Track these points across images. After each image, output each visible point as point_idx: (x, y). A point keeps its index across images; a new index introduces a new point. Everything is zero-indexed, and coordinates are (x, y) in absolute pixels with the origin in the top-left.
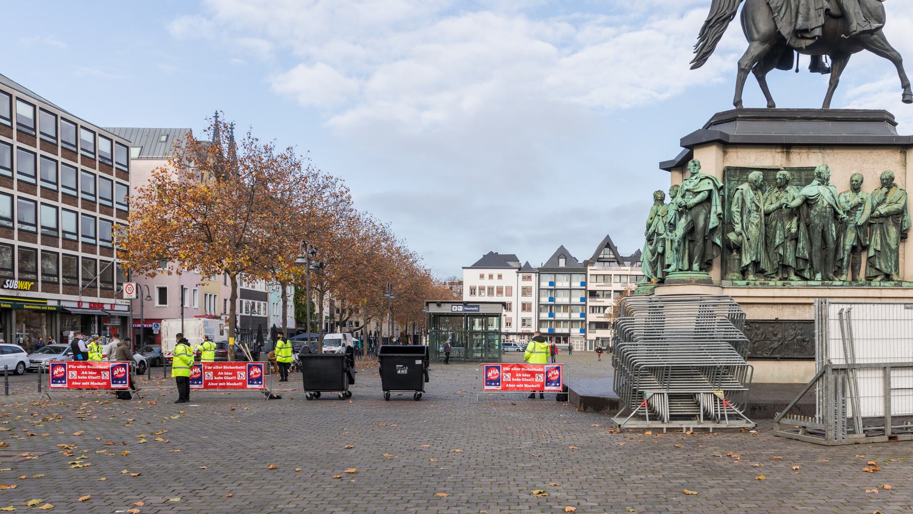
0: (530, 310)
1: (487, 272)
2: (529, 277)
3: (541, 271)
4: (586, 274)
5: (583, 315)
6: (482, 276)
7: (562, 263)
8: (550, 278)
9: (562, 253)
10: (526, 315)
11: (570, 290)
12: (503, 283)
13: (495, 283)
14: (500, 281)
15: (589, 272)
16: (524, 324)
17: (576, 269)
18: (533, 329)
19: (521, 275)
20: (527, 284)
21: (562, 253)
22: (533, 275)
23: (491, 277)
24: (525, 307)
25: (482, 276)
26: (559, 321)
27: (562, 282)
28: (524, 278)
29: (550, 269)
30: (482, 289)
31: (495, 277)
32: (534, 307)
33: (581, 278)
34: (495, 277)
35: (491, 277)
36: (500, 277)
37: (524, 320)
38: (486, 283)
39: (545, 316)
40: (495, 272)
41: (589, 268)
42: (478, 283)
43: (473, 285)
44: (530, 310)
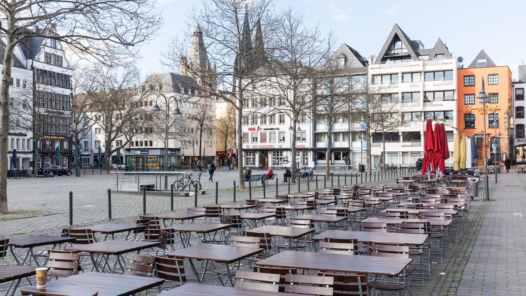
18: (308, 144)
26: (337, 134)
39: (322, 127)
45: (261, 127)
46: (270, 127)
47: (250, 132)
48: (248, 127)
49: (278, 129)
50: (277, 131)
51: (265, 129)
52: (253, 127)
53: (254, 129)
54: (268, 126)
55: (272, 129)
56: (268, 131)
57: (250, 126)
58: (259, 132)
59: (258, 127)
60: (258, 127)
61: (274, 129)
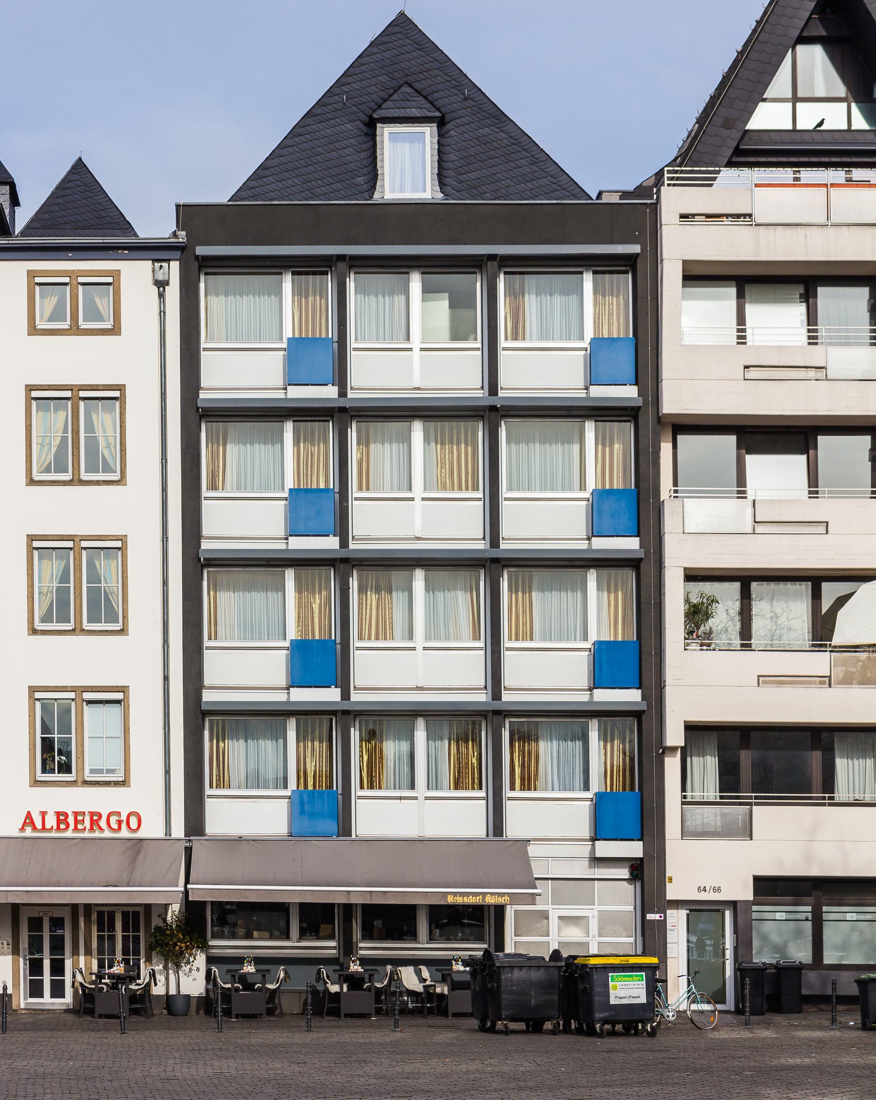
0: (105, 612)
3: (216, 245)
4: (637, 271)
5: (637, 659)
7: (407, 165)
8: (286, 306)
9: (402, 74)
10: (76, 660)
11: (491, 413)
15: (679, 244)
17: (516, 217)
21: (402, 74)
27: (409, 341)
29: (297, 218)
32: (149, 583)
33: (594, 307)
41: (674, 200)
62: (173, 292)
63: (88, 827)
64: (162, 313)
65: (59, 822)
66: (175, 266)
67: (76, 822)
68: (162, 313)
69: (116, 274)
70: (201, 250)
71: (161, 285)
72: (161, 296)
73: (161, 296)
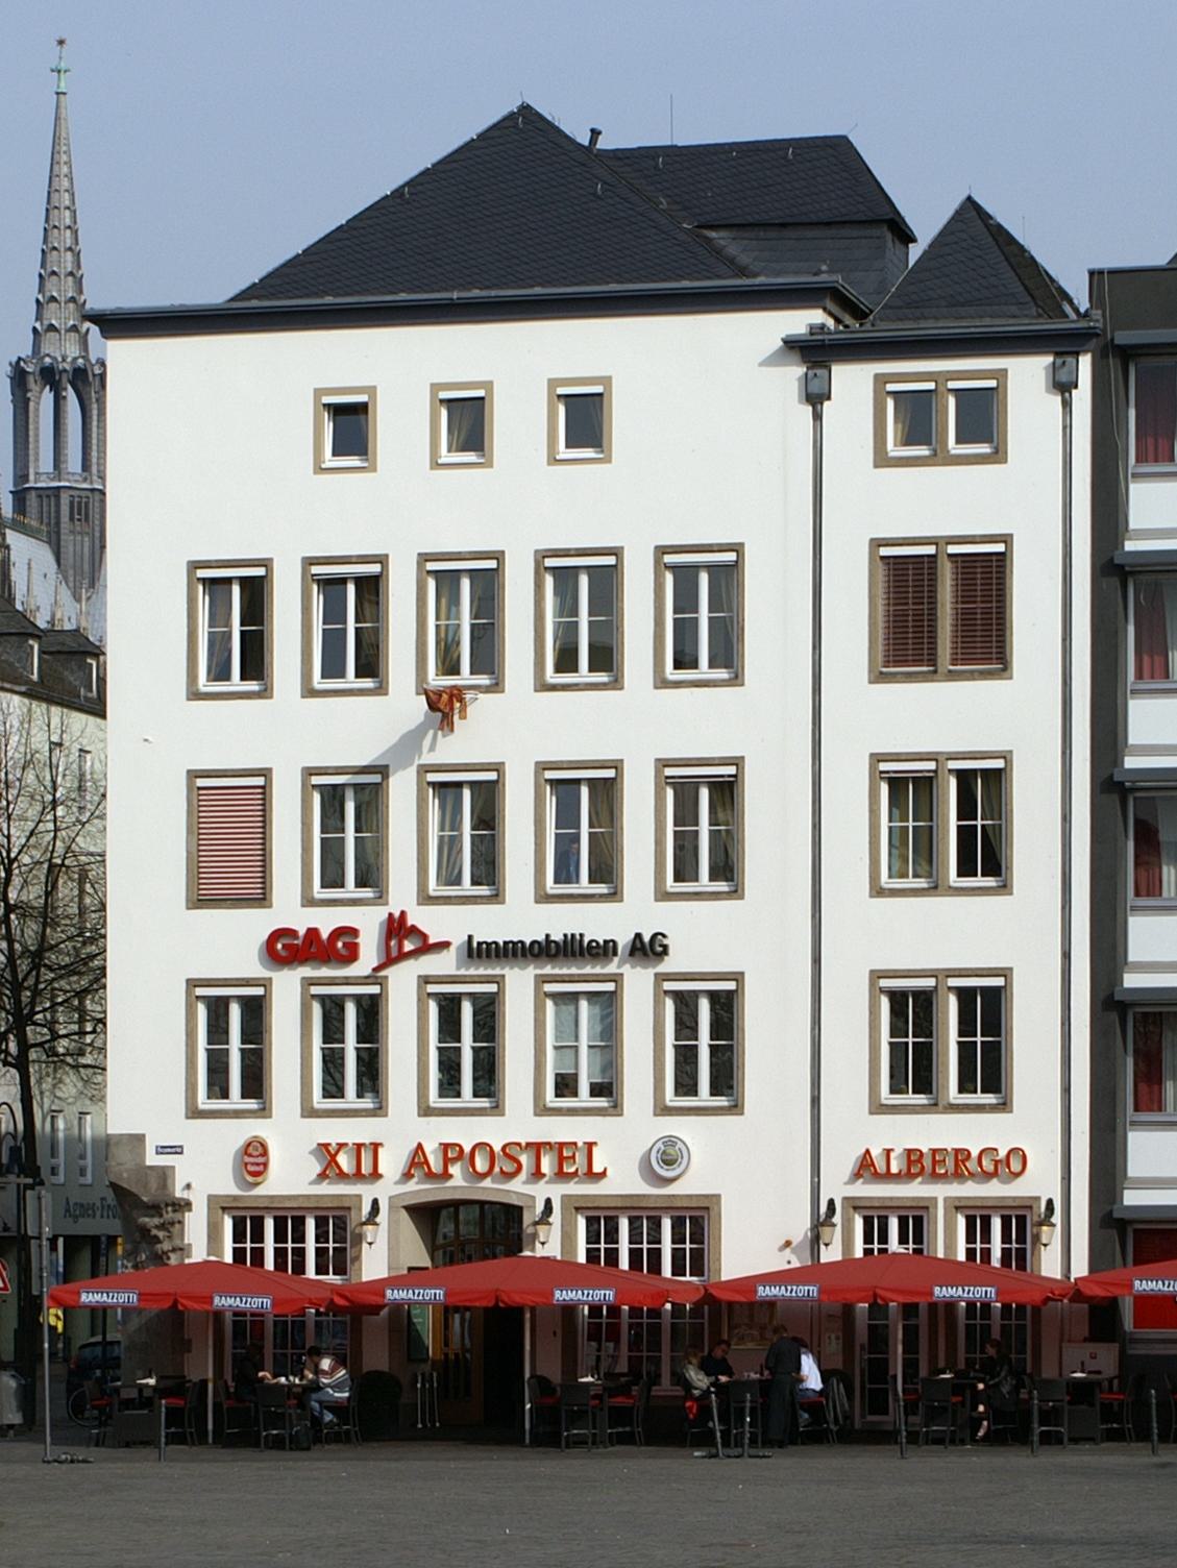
1: (402, 365)
2: (983, 419)
6: (350, 425)
12: (625, 510)
13: (524, 506)
14: (585, 476)
16: (913, 1071)
19: (853, 381)
20: (943, 504)
22: (1025, 377)
23: (468, 421)
24: (949, 822)
25: (350, 425)
28: (916, 418)
30: (353, 594)
31: (522, 422)
34: (522, 422)
35: (468, 421)
36: (585, 419)
37: (911, 1009)
38: (405, 509)
40: (519, 360)
42: (299, 518)
43: (231, 542)
44: (986, 857)
45: (433, 922)
46: (559, 922)
47: (287, 989)
48: (257, 924)
49: (648, 949)
50: (638, 983)
51: (478, 952)
52: (326, 921)
53: (337, 947)
54: (521, 916)
55: (572, 949)
56: (519, 985)
57: (289, 911)
58: (402, 983)
59: (397, 928)
60: (397, 928)
61: (606, 950)
62: (1083, 397)
63: (951, 1169)
64: (1067, 429)
65: (910, 1163)
66: (1085, 363)
67: (934, 1162)
68: (1067, 429)
69: (1000, 375)
70: (1123, 338)
71: (1063, 387)
72: (1067, 405)
73: (1067, 405)
